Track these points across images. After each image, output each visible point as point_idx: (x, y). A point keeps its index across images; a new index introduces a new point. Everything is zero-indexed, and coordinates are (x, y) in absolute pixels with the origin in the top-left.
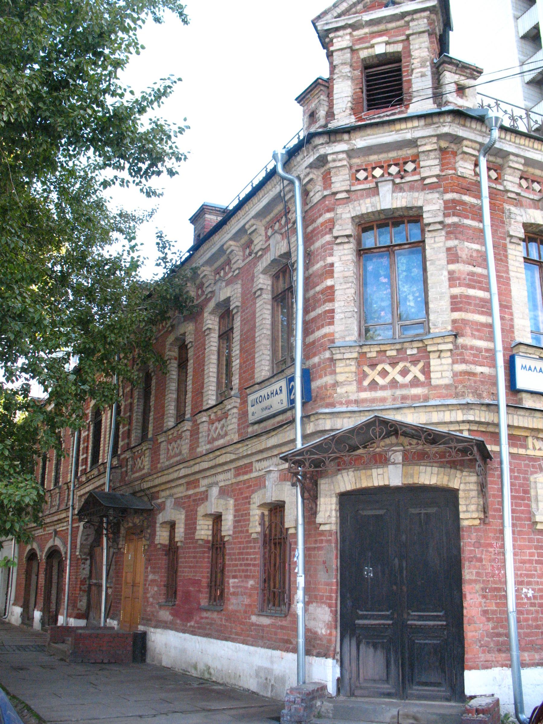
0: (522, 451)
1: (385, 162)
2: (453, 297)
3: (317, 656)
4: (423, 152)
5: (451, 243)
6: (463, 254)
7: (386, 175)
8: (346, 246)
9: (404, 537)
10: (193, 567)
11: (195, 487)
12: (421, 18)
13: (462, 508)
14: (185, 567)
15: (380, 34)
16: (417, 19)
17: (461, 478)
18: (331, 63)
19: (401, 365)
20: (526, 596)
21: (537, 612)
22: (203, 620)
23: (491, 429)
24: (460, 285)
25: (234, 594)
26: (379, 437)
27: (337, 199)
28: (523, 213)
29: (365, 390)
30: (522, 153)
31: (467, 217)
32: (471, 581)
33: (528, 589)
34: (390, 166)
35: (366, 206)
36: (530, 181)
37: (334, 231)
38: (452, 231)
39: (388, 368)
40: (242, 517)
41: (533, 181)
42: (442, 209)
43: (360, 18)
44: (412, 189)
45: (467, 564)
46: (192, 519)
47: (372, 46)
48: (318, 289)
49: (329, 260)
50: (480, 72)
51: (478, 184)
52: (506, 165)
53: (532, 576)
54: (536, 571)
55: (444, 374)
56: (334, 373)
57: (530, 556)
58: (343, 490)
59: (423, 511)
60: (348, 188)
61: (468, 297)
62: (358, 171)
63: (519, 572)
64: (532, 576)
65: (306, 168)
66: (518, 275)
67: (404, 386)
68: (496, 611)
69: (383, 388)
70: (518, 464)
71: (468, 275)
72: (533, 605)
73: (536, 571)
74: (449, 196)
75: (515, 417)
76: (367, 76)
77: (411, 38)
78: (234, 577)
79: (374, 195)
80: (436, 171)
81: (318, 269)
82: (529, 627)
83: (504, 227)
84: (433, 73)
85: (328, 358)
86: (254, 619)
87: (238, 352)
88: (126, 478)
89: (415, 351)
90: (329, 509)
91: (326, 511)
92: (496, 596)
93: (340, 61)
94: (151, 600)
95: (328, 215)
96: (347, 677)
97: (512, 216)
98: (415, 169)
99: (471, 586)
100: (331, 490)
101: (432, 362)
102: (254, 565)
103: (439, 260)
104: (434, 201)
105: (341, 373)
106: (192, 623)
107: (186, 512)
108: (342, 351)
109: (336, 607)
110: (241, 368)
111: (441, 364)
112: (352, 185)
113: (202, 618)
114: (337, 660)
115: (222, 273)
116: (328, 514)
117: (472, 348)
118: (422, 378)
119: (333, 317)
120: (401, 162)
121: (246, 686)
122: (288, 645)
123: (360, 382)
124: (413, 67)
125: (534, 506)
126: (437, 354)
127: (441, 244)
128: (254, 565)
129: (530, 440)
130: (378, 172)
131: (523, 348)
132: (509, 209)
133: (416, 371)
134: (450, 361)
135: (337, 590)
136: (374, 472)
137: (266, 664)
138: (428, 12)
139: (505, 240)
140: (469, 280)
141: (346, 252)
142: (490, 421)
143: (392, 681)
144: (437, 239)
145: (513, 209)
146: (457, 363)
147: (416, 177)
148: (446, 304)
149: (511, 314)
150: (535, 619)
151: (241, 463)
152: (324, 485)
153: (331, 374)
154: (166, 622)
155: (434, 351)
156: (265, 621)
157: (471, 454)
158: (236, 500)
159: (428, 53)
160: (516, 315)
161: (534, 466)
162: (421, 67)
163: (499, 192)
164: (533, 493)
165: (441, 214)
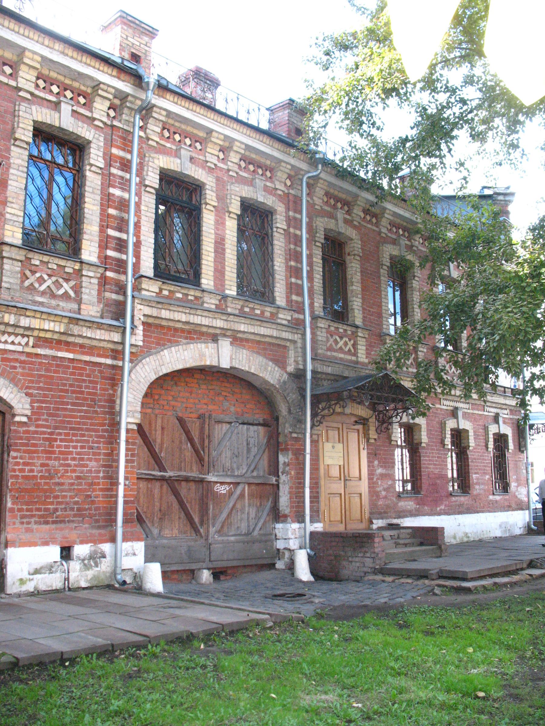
78: (476, 473)
106: (443, 507)
121: (493, 535)
137: (505, 520)
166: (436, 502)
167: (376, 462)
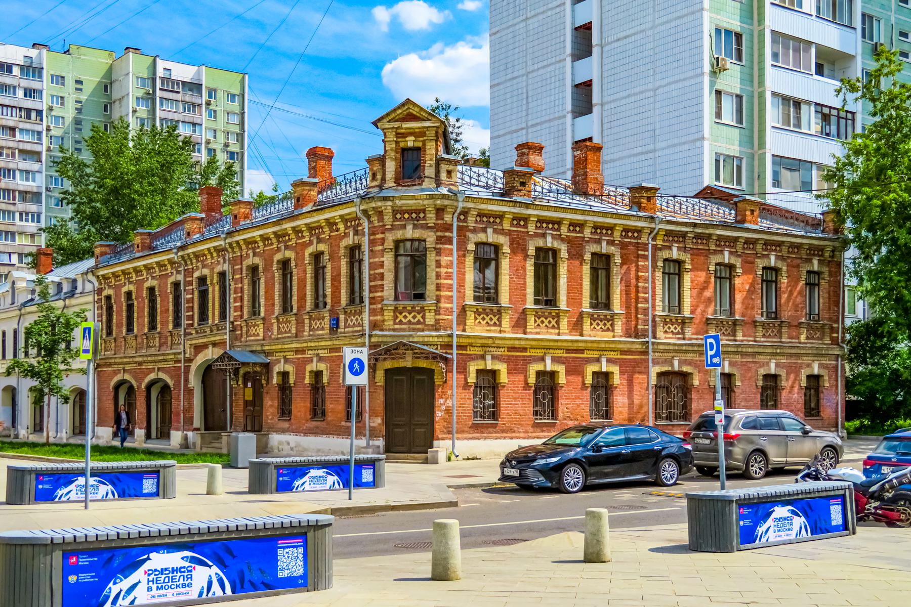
0: (464, 352)
2: (437, 284)
5: (438, 258)
15: (411, 134)
35: (399, 234)
48: (377, 271)
49: (382, 259)
51: (452, 225)
56: (383, 315)
67: (414, 324)
69: (405, 324)
74: (439, 234)
86: (343, 423)
123: (395, 320)
133: (419, 317)
145: (471, 235)
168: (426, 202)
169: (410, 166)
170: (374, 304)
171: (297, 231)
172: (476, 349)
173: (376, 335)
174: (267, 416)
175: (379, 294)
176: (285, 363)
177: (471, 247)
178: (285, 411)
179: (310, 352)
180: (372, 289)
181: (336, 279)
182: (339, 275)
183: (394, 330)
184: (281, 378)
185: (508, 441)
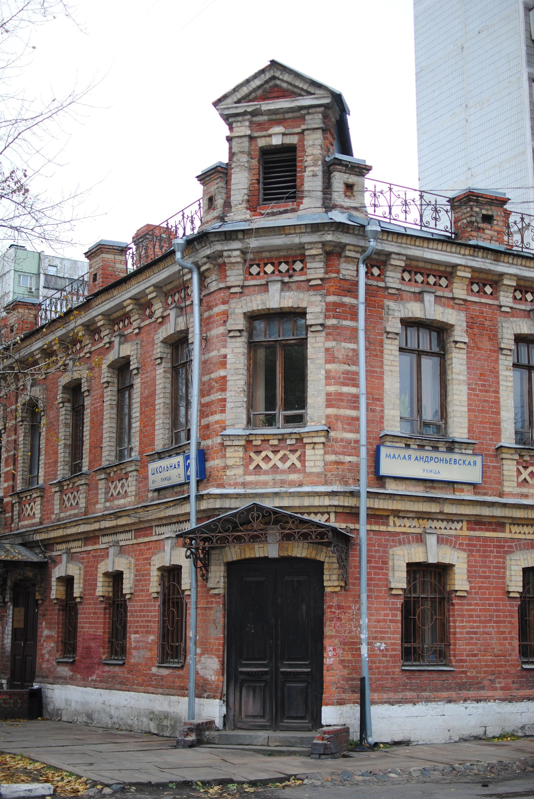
0: (383, 528)
1: (276, 258)
2: (328, 394)
3: (207, 698)
4: (310, 256)
5: (330, 344)
6: (340, 355)
7: (277, 272)
8: (238, 339)
9: (279, 600)
10: (94, 623)
11: (95, 543)
12: (316, 113)
13: (326, 577)
14: (85, 623)
15: (279, 122)
16: (313, 113)
17: (326, 553)
18: (230, 148)
19: (281, 453)
20: (380, 650)
21: (388, 661)
22: (105, 674)
23: (354, 511)
24: (335, 385)
25: (136, 648)
26: (257, 520)
27: (231, 293)
28: (402, 308)
29: (251, 474)
30: (403, 252)
31: (345, 319)
32: (332, 637)
33: (381, 643)
34: (280, 263)
35: (257, 302)
36: (413, 273)
37: (228, 324)
38: (333, 333)
39: (271, 455)
40: (141, 576)
41: (416, 273)
42: (324, 311)
43: (259, 107)
44: (299, 288)
45: (328, 623)
46: (91, 575)
47: (270, 136)
48: (213, 376)
49: (223, 351)
50: (368, 169)
52: (388, 263)
53: (386, 632)
54: (390, 628)
55: (317, 463)
56: (224, 456)
57: (384, 616)
58: (230, 560)
59: (296, 579)
60: (241, 283)
61: (341, 394)
62: (251, 266)
63: (374, 630)
64: (386, 632)
65: (204, 257)
66: (393, 368)
67: (283, 472)
68: (351, 660)
69: (266, 473)
70: (379, 539)
71: (343, 373)
72: (385, 656)
73: (390, 628)
74: (331, 299)
75: (376, 500)
76: (266, 163)
77: (306, 133)
78: (136, 632)
79: (265, 292)
80: (321, 274)
81: (213, 357)
82: (380, 673)
83: (382, 323)
84: (324, 172)
85: (220, 443)
86: (154, 670)
87: (138, 414)
88: (13, 526)
89: (294, 442)
90: (218, 575)
91: (216, 577)
92: (352, 648)
93: (239, 149)
94: (47, 656)
95: (222, 308)
96: (232, 714)
97: (391, 312)
98: (302, 269)
99: (331, 640)
100: (219, 560)
101: (309, 452)
102: (154, 622)
103: (318, 359)
104: (317, 304)
105: (230, 457)
106: (94, 677)
107: (86, 567)
108: (232, 438)
109: (223, 657)
110: (141, 431)
111: (315, 455)
112: (246, 279)
113: (104, 672)
114: (224, 701)
115: (121, 325)
116: (217, 580)
117: (342, 440)
118: (298, 465)
119: (225, 406)
120: (290, 260)
122: (182, 691)
123: (246, 466)
124: (306, 164)
125: (390, 574)
126: (312, 446)
127: (321, 345)
128: (154, 622)
129: (391, 519)
130: (269, 269)
131: (388, 439)
132: (388, 306)
133: (293, 458)
134: (322, 452)
135: (224, 643)
136: (256, 546)
138: (323, 108)
139: (382, 336)
140: (344, 378)
141: (238, 345)
142: (353, 505)
143: (267, 717)
144: (317, 339)
145: (391, 304)
146: (328, 453)
147: (303, 278)
148: (321, 400)
149: (382, 406)
150: (386, 667)
151: (142, 526)
152: (215, 555)
153: (222, 457)
154: (65, 678)
155: (310, 443)
156: (165, 672)
157: (327, 538)
158: (137, 560)
159: (320, 151)
160: (386, 406)
161: (393, 540)
162: (313, 166)
163: (380, 289)
164: (390, 563)
165: (322, 316)
166: (89, 670)
167: (44, 624)
168: (306, 239)
169: (277, 174)
170: (209, 437)
171: (91, 329)
172: (407, 522)
173: (210, 496)
174: (42, 655)
175: (217, 417)
176: (68, 562)
177: (394, 325)
178: (69, 644)
179: (105, 539)
180: (205, 411)
181: (148, 402)
182: (153, 394)
183: (244, 485)
184: (62, 589)
185: (472, 706)
